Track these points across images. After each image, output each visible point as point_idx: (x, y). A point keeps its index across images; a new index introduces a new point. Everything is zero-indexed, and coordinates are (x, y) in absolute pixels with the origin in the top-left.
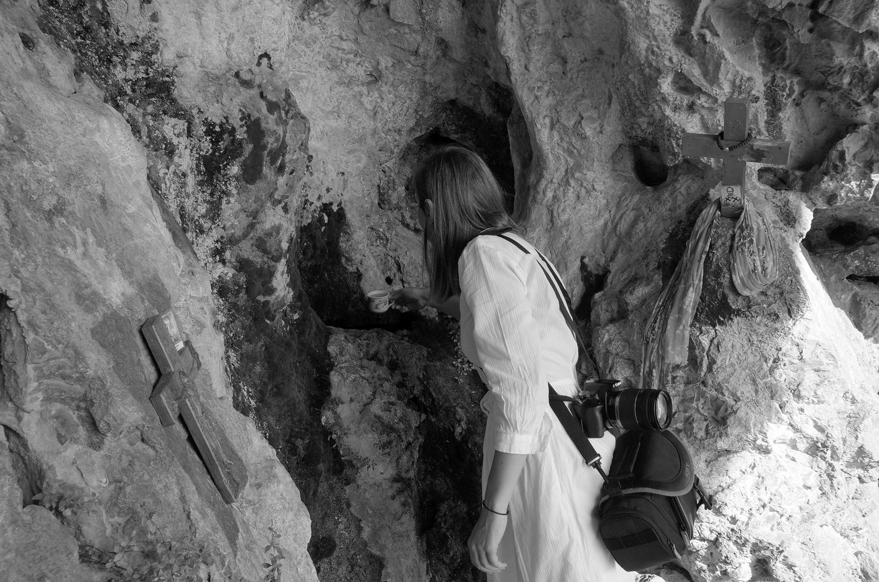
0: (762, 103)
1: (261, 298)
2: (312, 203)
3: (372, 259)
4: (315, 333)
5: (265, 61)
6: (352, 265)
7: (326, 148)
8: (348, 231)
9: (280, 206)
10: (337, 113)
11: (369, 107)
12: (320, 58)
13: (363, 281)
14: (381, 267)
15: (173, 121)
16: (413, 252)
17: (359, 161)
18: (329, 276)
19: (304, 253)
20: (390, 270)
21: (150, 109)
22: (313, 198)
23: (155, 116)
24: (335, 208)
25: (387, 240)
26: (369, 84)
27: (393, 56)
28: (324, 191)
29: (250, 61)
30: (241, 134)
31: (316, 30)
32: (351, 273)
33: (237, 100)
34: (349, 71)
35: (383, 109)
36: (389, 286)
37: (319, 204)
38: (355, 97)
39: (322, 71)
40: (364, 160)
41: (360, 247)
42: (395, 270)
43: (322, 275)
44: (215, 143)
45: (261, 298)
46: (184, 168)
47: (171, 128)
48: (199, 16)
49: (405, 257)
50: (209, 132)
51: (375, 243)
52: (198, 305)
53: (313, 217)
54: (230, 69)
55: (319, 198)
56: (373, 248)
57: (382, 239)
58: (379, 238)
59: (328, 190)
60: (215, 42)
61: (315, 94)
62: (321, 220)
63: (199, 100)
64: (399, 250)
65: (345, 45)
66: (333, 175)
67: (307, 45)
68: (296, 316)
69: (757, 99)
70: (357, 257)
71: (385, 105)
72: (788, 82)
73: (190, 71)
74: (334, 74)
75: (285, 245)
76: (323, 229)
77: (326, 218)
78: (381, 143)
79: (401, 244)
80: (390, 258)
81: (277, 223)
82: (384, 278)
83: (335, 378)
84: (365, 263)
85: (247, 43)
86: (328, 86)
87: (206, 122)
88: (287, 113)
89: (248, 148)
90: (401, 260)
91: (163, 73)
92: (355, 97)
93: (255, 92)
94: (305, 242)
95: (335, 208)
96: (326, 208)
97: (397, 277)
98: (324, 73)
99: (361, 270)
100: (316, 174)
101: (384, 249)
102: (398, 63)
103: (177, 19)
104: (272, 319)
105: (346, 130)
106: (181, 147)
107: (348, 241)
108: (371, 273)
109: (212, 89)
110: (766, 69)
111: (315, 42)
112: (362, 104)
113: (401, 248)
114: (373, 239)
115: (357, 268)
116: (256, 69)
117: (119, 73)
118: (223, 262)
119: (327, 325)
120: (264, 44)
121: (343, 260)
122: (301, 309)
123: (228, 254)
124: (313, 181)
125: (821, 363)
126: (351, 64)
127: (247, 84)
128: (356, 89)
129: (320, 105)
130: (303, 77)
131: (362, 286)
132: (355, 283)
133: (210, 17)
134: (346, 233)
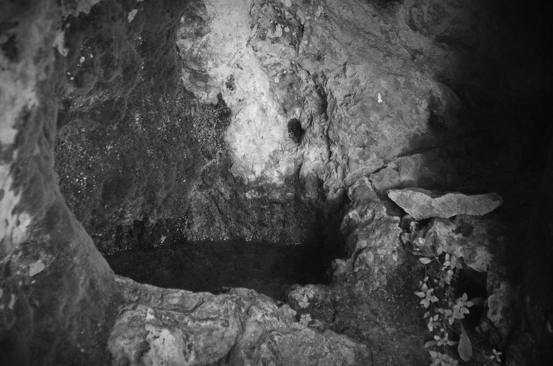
3: (259, 73)
4: (83, 301)
6: (207, 89)
8: (200, 13)
13: (232, 128)
14: (281, 94)
16: (360, 68)
18: (145, 121)
19: (78, 83)
20: (301, 103)
25: (302, 29)
32: (204, 106)
36: (292, 145)
42: (312, 107)
43: (129, 118)
49: (341, 80)
51: (269, 34)
56: (265, 46)
57: (289, 25)
58: (281, 20)
64: (327, 57)
79: (335, 44)
80: (303, 75)
82: (283, 122)
84: (239, 84)
90: (330, 85)
94: (83, 53)
97: (316, 128)
99: (229, 100)
101: (292, 52)
107: (199, 34)
108: (252, 111)
113: (333, 54)
114: (267, 23)
115: (220, 96)
119: (119, 272)
121: (185, 77)
122: (50, 250)
131: (228, 139)
132: (213, 132)
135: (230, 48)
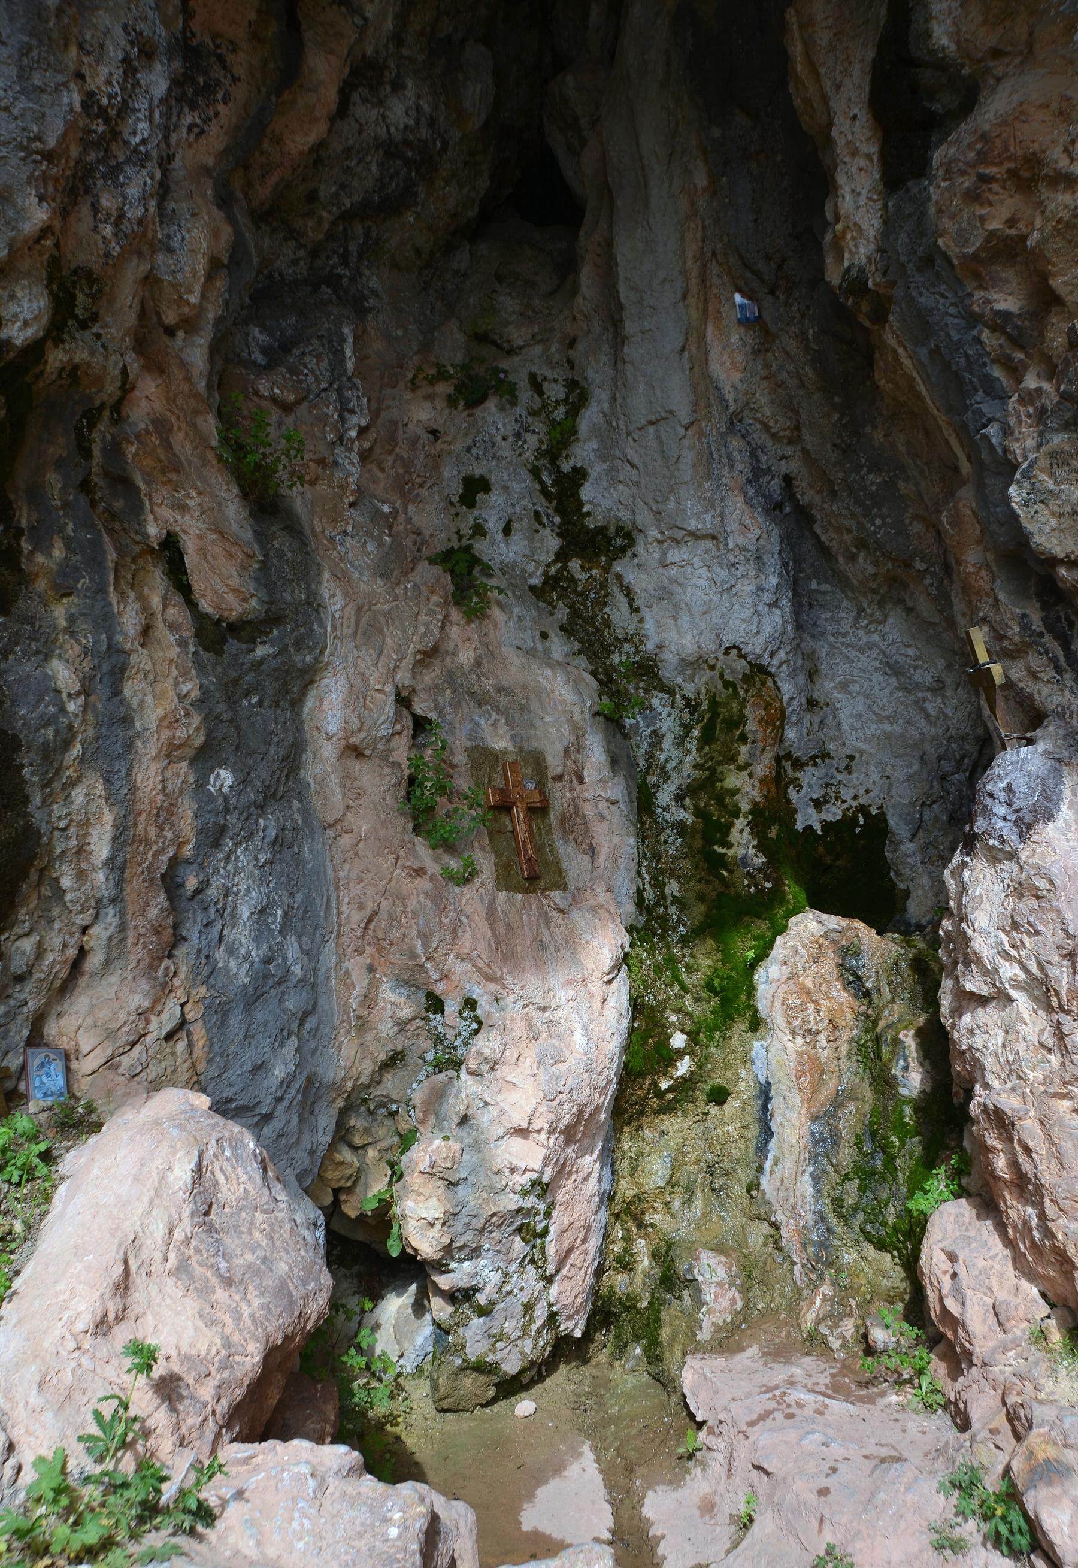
0: (1048, 639)
1: (719, 850)
2: (844, 802)
5: (734, 652)
7: (872, 751)
9: (745, 773)
10: (893, 718)
11: (933, 713)
12: (877, 664)
15: (661, 695)
17: (909, 766)
21: (642, 684)
22: (846, 794)
23: (647, 691)
24: (874, 812)
26: (933, 691)
27: (943, 657)
28: (862, 792)
29: (717, 651)
30: (705, 706)
31: (876, 637)
33: (704, 680)
34: (917, 678)
35: (946, 716)
37: (855, 804)
38: (916, 702)
39: (878, 677)
40: (916, 767)
41: (910, 860)
44: (692, 714)
45: (719, 850)
46: (664, 730)
47: (658, 701)
48: (675, 618)
50: (688, 705)
52: (606, 804)
53: (844, 814)
54: (700, 657)
55: (855, 797)
59: (867, 791)
60: (689, 637)
61: (867, 697)
62: (854, 821)
63: (679, 680)
65: (910, 652)
66: (875, 777)
67: (861, 650)
68: (768, 885)
69: (1041, 635)
70: (906, 871)
71: (949, 711)
72: (1062, 614)
73: (670, 657)
74: (894, 679)
75: (745, 806)
76: (858, 830)
77: (861, 820)
78: (942, 750)
81: (739, 785)
83: (779, 940)
85: (713, 637)
86: (887, 691)
87: (685, 698)
88: (747, 691)
89: (708, 715)
91: (648, 659)
92: (916, 702)
93: (716, 673)
95: (874, 811)
96: (863, 809)
98: (881, 678)
100: (854, 775)
102: (949, 666)
103: (657, 622)
104: (730, 872)
105: (902, 735)
106: (664, 715)
107: (895, 851)
108: (920, 893)
109: (689, 672)
110: (1045, 606)
111: (871, 649)
112: (923, 710)
114: (934, 858)
116: (721, 656)
117: (616, 659)
118: (683, 806)
120: (729, 638)
121: (892, 874)
123: (687, 801)
124: (850, 781)
125: (1037, 888)
126: (919, 671)
127: (712, 668)
128: (920, 695)
129: (875, 708)
130: (853, 681)
133: (685, 619)
134: (892, 842)
135: (910, 860)
